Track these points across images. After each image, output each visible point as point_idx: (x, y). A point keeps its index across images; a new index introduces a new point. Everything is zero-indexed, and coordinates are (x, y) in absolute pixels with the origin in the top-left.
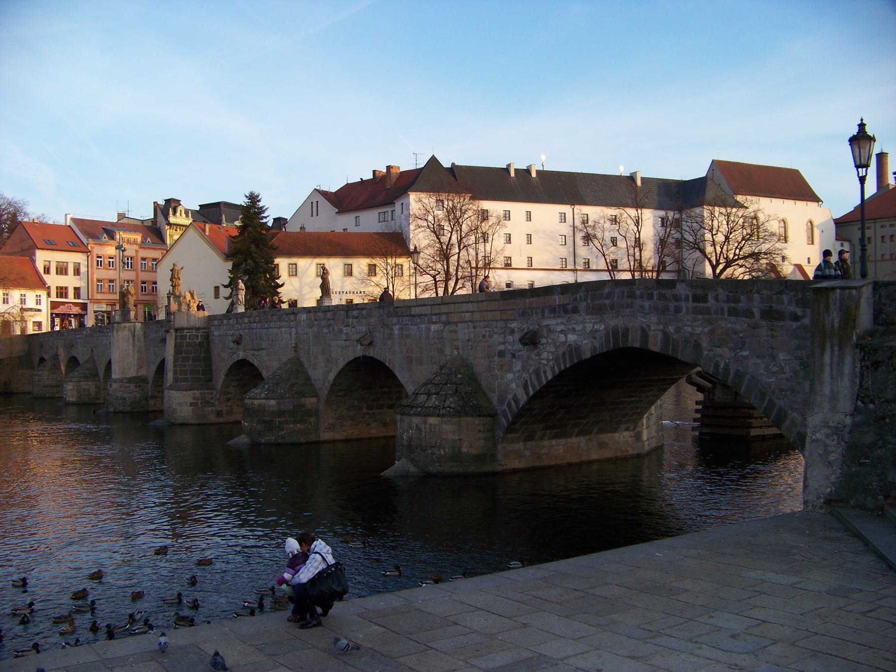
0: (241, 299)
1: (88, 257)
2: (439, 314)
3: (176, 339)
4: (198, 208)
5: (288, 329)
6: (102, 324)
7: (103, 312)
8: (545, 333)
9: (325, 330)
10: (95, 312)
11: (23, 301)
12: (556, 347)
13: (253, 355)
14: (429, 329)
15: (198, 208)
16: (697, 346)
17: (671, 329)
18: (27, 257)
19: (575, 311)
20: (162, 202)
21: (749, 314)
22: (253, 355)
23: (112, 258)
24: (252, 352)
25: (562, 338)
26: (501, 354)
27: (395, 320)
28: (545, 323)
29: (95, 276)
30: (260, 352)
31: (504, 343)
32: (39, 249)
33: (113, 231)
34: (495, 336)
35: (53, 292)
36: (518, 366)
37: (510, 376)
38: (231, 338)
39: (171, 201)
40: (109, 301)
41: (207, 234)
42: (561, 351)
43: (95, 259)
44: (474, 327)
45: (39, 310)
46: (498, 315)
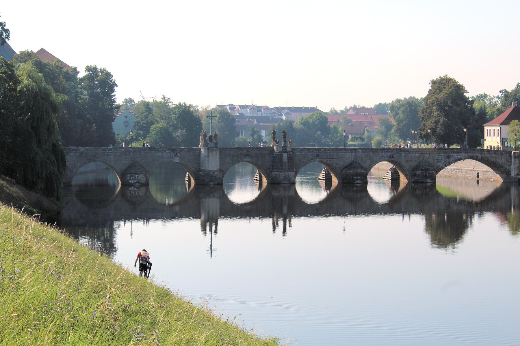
2: (419, 152)
3: (288, 155)
5: (351, 153)
8: (452, 156)
9: (371, 154)
12: (455, 158)
13: (327, 160)
14: (415, 155)
16: (488, 158)
17: (483, 156)
19: (461, 152)
21: (498, 154)
22: (327, 160)
24: (327, 159)
25: (457, 157)
26: (437, 159)
27: (403, 152)
28: (452, 154)
30: (332, 159)
31: (438, 158)
34: (436, 157)
36: (443, 161)
37: (440, 163)
38: (310, 155)
42: (456, 159)
44: (430, 154)
46: (437, 152)
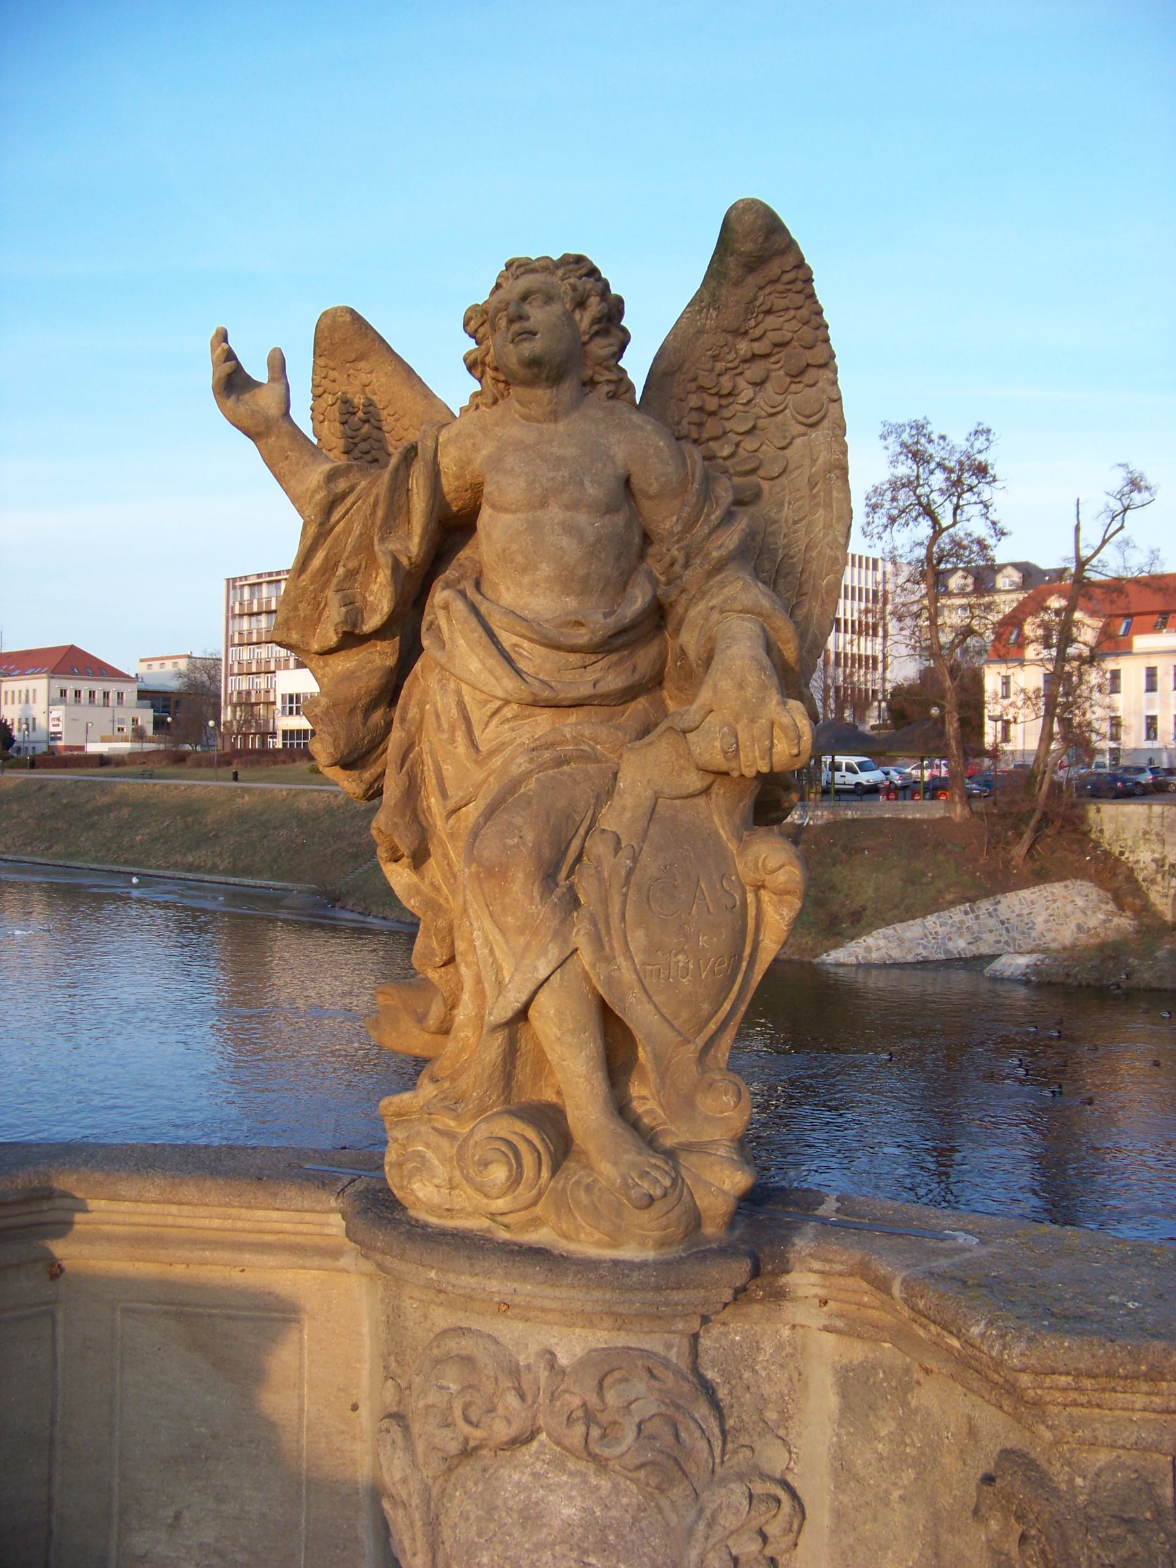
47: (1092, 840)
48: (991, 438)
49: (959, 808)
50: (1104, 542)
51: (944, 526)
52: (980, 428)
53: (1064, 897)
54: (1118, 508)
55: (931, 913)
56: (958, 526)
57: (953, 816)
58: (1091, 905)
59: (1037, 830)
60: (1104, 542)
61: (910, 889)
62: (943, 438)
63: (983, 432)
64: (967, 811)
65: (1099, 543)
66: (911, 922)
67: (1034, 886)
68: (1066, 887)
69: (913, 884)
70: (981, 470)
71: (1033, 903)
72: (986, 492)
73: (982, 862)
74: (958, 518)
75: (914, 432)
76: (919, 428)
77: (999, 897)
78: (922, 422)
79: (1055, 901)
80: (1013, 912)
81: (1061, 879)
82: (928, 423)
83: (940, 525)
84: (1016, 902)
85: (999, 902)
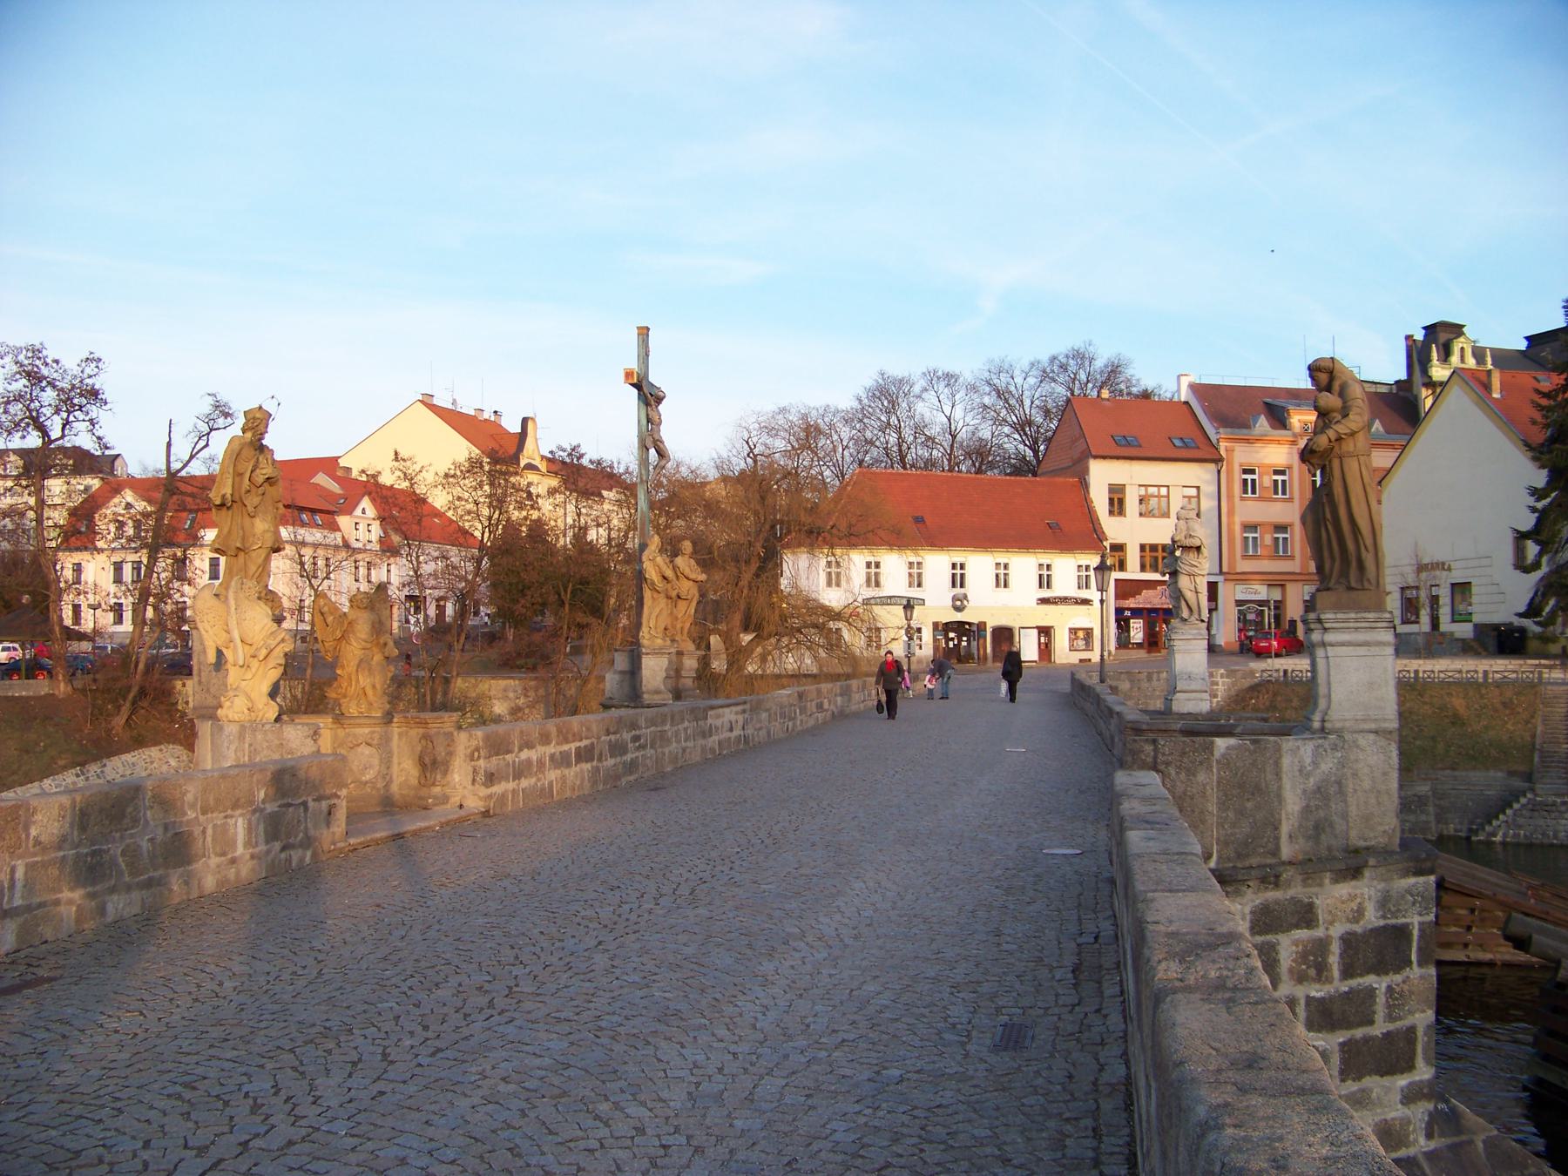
0: (1189, 595)
1: (1219, 472)
4: (1523, 345)
6: (1256, 631)
7: (1261, 603)
10: (1239, 603)
11: (1045, 581)
15: (1523, 345)
18: (1073, 476)
20: (1419, 336)
23: (1282, 473)
29: (1238, 520)
32: (1096, 457)
33: (1283, 408)
35: (1133, 557)
39: (1438, 329)
40: (1270, 577)
41: (1496, 395)
43: (1238, 477)
45: (1086, 602)
47: (179, 711)
48: (100, 365)
49: (62, 685)
50: (192, 457)
51: (53, 438)
52: (92, 356)
53: (160, 759)
54: (205, 429)
55: (47, 777)
56: (66, 439)
57: (57, 693)
58: (182, 765)
59: (134, 703)
60: (192, 457)
61: (26, 757)
62: (57, 362)
63: (92, 360)
64: (69, 688)
65: (187, 458)
66: (29, 785)
67: (134, 751)
68: (161, 750)
69: (27, 752)
70: (94, 394)
71: (134, 764)
72: (94, 411)
73: (86, 731)
74: (66, 432)
75: (30, 355)
76: (36, 352)
77: (104, 761)
78: (38, 346)
79: (152, 762)
80: (118, 773)
81: (156, 743)
82: (44, 348)
83: (49, 436)
84: (120, 765)
85: (105, 765)
